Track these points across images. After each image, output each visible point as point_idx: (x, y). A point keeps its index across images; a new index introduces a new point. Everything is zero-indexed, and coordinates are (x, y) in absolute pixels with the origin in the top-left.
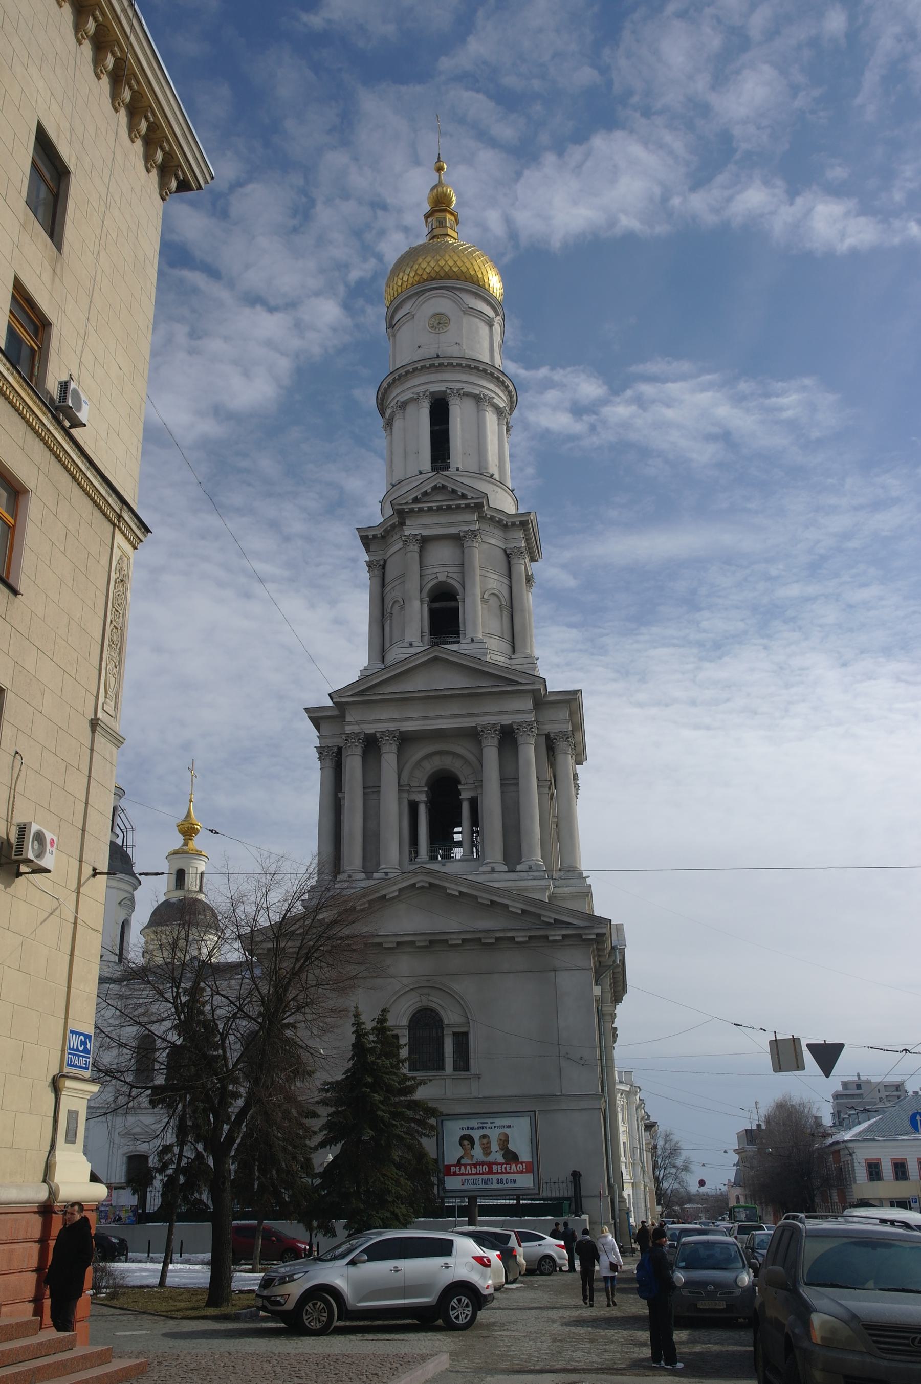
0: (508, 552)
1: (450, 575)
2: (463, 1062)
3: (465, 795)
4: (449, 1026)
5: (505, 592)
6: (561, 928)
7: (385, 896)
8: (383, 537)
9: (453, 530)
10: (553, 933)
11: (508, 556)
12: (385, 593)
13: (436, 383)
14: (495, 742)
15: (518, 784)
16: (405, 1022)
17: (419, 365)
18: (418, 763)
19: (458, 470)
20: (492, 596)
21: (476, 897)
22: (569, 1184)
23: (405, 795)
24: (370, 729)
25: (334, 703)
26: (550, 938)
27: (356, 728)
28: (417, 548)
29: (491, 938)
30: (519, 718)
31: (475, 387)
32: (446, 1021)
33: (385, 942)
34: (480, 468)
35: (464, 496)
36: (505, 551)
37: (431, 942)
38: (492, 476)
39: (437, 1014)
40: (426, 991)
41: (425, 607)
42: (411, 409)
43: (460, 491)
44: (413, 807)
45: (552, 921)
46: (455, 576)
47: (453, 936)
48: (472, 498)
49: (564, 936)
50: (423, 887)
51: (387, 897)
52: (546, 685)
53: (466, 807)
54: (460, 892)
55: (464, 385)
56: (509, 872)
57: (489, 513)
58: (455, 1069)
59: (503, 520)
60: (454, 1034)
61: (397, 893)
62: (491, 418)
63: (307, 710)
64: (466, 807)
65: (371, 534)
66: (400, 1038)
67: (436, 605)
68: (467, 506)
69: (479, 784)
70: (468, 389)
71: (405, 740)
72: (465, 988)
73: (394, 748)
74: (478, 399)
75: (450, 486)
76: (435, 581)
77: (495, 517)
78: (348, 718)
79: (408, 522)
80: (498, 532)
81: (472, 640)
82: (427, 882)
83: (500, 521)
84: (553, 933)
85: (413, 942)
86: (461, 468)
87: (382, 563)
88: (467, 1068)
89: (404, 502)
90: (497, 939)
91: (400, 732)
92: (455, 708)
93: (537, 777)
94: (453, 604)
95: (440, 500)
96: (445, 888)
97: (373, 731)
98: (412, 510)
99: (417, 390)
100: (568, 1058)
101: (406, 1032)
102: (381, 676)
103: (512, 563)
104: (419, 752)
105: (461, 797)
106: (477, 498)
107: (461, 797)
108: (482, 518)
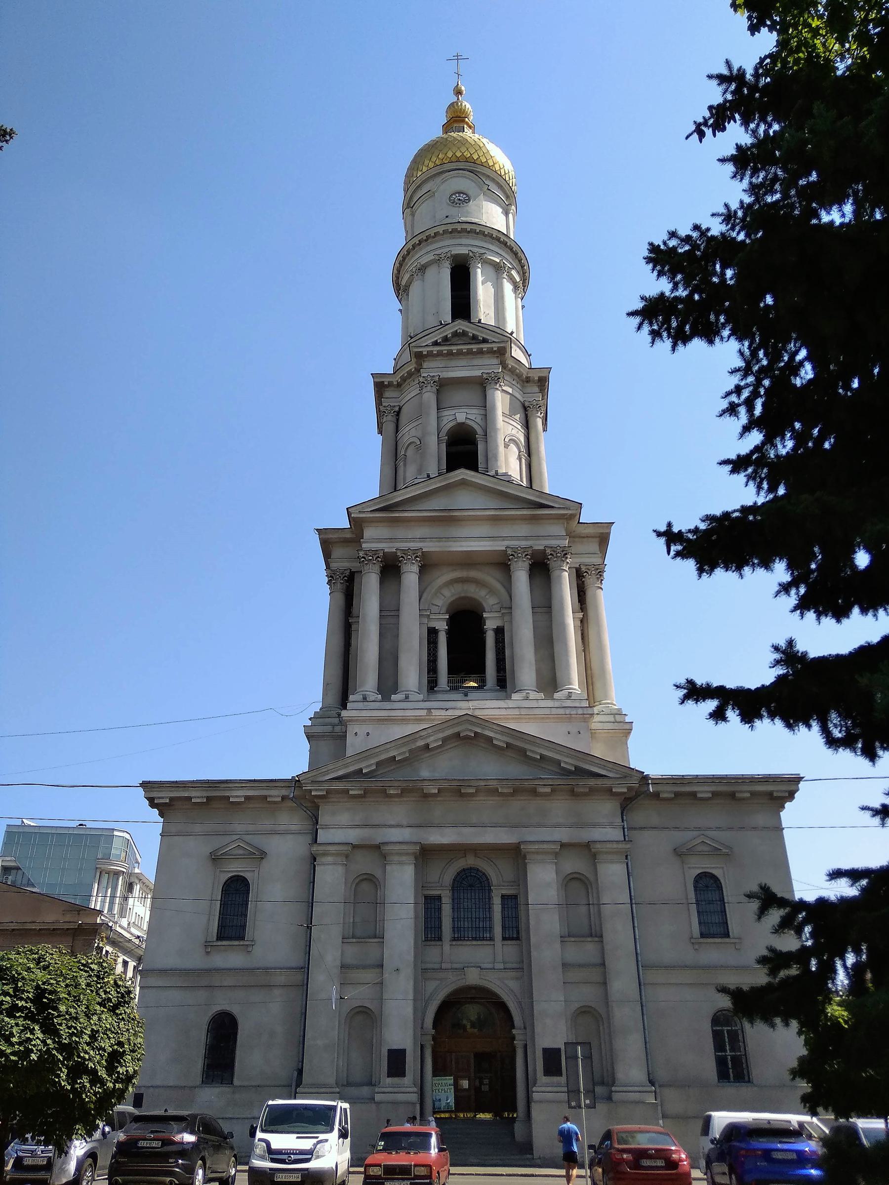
0: (527, 404)
3: (491, 624)
5: (522, 438)
8: (399, 385)
11: (525, 409)
12: (398, 438)
30: (554, 543)
35: (485, 341)
43: (481, 335)
44: (432, 633)
65: (386, 381)
68: (491, 352)
69: (507, 609)
73: (415, 568)
75: (471, 330)
87: (397, 409)
94: (469, 447)
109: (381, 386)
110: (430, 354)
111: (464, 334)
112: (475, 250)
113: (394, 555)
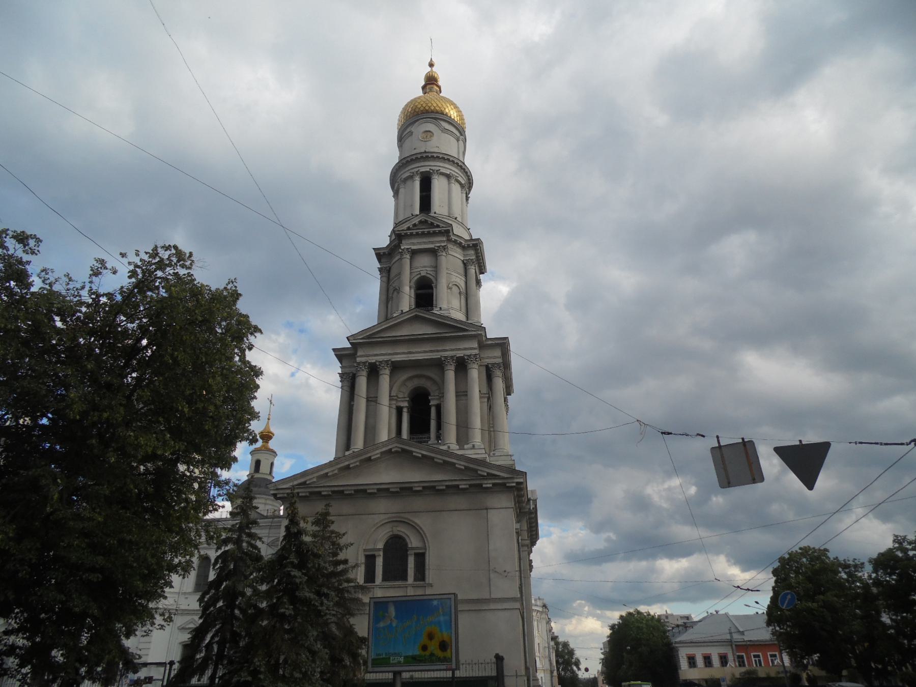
0: (465, 262)
1: (428, 272)
2: (421, 573)
3: (432, 403)
4: (413, 548)
5: (463, 285)
6: (491, 479)
7: (370, 457)
10: (486, 482)
13: (425, 167)
14: (453, 368)
15: (467, 395)
16: (380, 546)
19: (435, 213)
20: (455, 286)
21: (433, 458)
22: (493, 665)
23: (394, 402)
24: (372, 360)
25: (351, 343)
26: (484, 486)
27: (363, 359)
28: (408, 256)
29: (442, 485)
30: (468, 352)
31: (447, 170)
32: (410, 546)
33: (369, 489)
34: (449, 213)
35: (438, 226)
36: (463, 261)
37: (401, 489)
38: (456, 219)
39: (404, 540)
40: (396, 524)
41: (413, 291)
42: (409, 183)
43: (436, 223)
44: (399, 411)
45: (486, 474)
46: (431, 273)
47: (416, 485)
48: (443, 227)
49: (494, 484)
50: (396, 452)
51: (372, 458)
52: (486, 332)
53: (433, 410)
54: (423, 455)
55: (440, 168)
56: (460, 449)
57: (453, 238)
58: (415, 580)
59: (462, 243)
60: (416, 555)
61: (379, 456)
62: (456, 188)
63: (334, 350)
64: (433, 410)
65: (382, 252)
66: (377, 557)
67: (420, 292)
69: (442, 396)
70: (443, 170)
71: (396, 367)
72: (422, 521)
73: (387, 371)
74: (448, 177)
75: (430, 220)
76: (419, 276)
77: (457, 240)
78: (359, 354)
79: (403, 242)
80: (459, 250)
81: (441, 308)
82: (399, 447)
83: (460, 244)
84: (486, 482)
85: (388, 489)
86: (437, 212)
87: (388, 268)
88: (423, 579)
89: (402, 229)
90: (446, 486)
91: (392, 362)
93: (480, 391)
94: (430, 291)
96: (411, 452)
97: (374, 361)
98: (406, 234)
99: (413, 171)
100: (496, 572)
101: (381, 553)
102: (382, 326)
103: (467, 268)
104: (404, 376)
105: (430, 404)
106: (446, 227)
107: (430, 404)
109: (381, 255)
110: (406, 235)
111: (426, 221)
112: (433, 168)
113: (375, 363)
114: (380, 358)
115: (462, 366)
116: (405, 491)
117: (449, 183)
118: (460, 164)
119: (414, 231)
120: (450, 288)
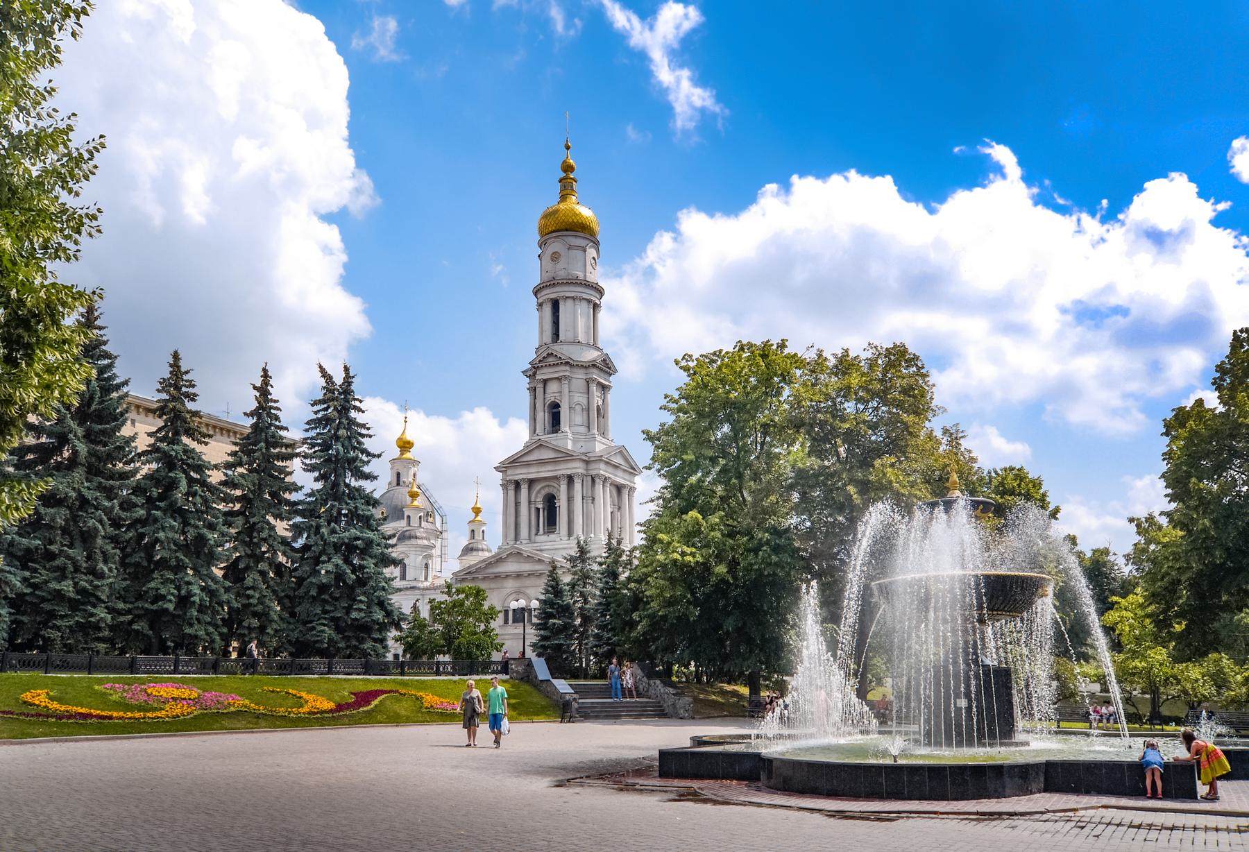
5: (584, 401)
9: (556, 375)
17: (544, 285)
18: (539, 491)
24: (516, 478)
30: (574, 471)
42: (544, 305)
43: (559, 356)
44: (538, 509)
57: (575, 363)
65: (528, 374)
67: (554, 410)
71: (531, 482)
73: (526, 486)
75: (554, 353)
80: (582, 371)
83: (582, 366)
92: (549, 468)
95: (551, 359)
104: (537, 487)
108: (571, 366)
114: (521, 477)
115: (570, 479)
116: (518, 576)
117: (575, 305)
118: (583, 282)
119: (544, 364)
120: (574, 409)
